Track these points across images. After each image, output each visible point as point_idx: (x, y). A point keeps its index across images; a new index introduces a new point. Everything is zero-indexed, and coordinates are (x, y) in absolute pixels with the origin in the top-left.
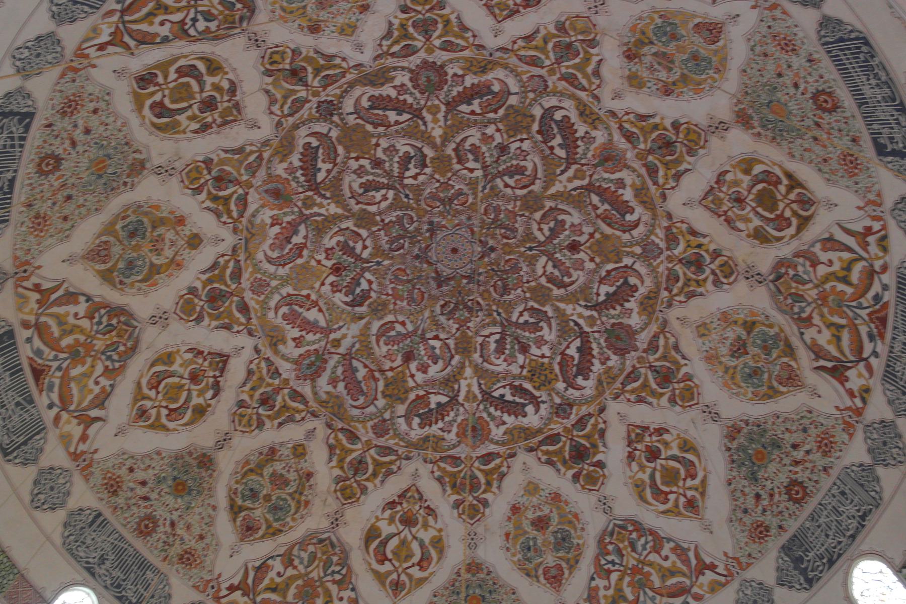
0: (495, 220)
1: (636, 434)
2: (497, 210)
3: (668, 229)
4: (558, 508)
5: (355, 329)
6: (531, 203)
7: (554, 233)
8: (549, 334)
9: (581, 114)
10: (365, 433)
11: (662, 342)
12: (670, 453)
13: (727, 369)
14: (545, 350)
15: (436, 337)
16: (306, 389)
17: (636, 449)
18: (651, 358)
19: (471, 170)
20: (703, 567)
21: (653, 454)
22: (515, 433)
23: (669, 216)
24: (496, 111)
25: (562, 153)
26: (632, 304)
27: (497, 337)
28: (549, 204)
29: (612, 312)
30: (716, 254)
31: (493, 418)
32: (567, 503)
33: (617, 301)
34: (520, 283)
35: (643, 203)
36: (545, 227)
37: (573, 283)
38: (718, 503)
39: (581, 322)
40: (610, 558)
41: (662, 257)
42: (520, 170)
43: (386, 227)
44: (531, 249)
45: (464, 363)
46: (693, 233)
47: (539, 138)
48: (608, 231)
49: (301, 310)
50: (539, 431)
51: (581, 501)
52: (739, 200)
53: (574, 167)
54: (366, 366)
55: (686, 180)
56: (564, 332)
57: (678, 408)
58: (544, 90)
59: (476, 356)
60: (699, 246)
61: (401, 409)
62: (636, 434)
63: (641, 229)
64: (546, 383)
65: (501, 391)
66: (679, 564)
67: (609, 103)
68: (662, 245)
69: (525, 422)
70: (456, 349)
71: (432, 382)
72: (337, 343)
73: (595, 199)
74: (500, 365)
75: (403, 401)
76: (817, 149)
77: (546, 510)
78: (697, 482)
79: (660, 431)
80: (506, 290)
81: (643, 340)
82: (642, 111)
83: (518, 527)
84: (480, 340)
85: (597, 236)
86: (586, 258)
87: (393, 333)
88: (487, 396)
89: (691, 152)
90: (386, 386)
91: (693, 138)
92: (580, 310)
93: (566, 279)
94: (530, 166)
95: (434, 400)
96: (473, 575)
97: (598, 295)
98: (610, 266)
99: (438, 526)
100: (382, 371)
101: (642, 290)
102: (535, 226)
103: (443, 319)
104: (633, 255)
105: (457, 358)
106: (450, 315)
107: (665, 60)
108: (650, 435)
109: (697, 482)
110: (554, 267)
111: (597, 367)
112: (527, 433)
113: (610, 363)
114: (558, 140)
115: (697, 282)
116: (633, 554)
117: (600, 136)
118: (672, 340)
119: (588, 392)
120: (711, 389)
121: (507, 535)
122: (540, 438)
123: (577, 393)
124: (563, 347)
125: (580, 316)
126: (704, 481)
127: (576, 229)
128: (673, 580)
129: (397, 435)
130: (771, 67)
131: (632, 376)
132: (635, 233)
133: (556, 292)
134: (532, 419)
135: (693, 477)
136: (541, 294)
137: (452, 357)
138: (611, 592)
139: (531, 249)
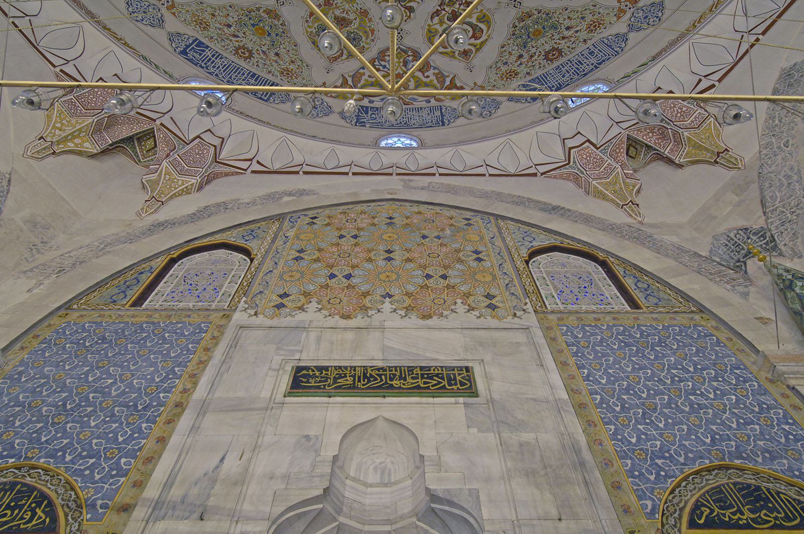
4: (362, 20)
17: (444, 9)
32: (370, 20)
40: (383, 63)
66: (435, 82)
77: (352, 16)
96: (269, 18)
108: (460, 5)
116: (403, 68)
126: (483, 43)
135: (476, 39)
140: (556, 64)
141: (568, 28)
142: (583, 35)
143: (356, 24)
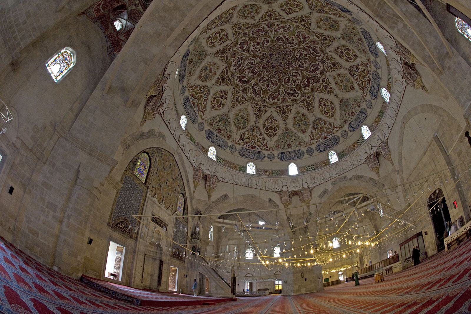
0: (280, 72)
1: (226, 92)
2: (282, 73)
3: (267, 106)
5: (272, 36)
6: (280, 81)
7: (272, 82)
8: (250, 74)
9: (295, 99)
10: (247, 31)
11: (244, 100)
12: (222, 101)
13: (238, 114)
14: (247, 73)
15: (259, 50)
16: (266, 22)
18: (241, 97)
19: (293, 73)
20: (203, 112)
21: (222, 97)
22: (231, 64)
23: (270, 107)
24: (303, 85)
25: (289, 91)
26: (253, 94)
27: (253, 63)
28: (279, 84)
29: (252, 90)
30: (261, 115)
31: (235, 59)
33: (254, 91)
34: (264, 71)
35: (274, 103)
36: (274, 81)
37: (260, 83)
38: (214, 113)
39: (251, 82)
40: (203, 89)
41: (261, 104)
42: (288, 82)
43: (291, 52)
44: (270, 76)
45: (250, 54)
46: (266, 111)
47: (293, 89)
48: (269, 94)
49: (285, 29)
50: (229, 69)
51: (213, 81)
52: (271, 123)
53: (285, 92)
54: (262, 34)
55: (276, 113)
56: (250, 78)
57: (231, 103)
58: (302, 95)
59: (251, 58)
60: (263, 112)
61: (247, 39)
62: (226, 92)
63: (268, 101)
64: (240, 72)
65: (241, 61)
67: (295, 105)
68: (264, 104)
69: (232, 66)
70: (255, 54)
71: (250, 46)
72: (271, 31)
73: (277, 94)
74: (247, 62)
75: (248, 40)
76: (280, 141)
78: (217, 108)
79: (226, 98)
80: (263, 68)
81: (245, 96)
82: (292, 111)
83: (211, 65)
84: (254, 59)
85: (269, 91)
86: (264, 87)
87: (266, 42)
88: (241, 58)
89: (281, 116)
90: (254, 37)
91: (285, 118)
92: (254, 83)
93: (261, 82)
94: (288, 84)
95: (245, 46)
97: (256, 87)
98: (261, 92)
99: (217, 46)
100: (258, 37)
101: (255, 97)
102: (275, 79)
103: (263, 53)
104: (263, 98)
105: (252, 53)
106: (263, 55)
107: (300, 120)
109: (217, 108)
110: (265, 80)
111: (241, 84)
112: (230, 66)
113: (241, 87)
114: (291, 92)
115: (256, 110)
117: (289, 100)
118: (244, 102)
119: (235, 81)
120: (235, 110)
121: (210, 63)
122: (228, 70)
123: (236, 79)
124: (246, 77)
125: (252, 83)
127: (271, 87)
128: (200, 106)
129: (242, 37)
130: (296, 139)
131: (238, 92)
132: (268, 99)
133: (259, 79)
134: (232, 68)
136: (259, 75)
137: (253, 52)
138: (197, 91)
139: (270, 76)
140: (218, 134)
141: (227, 129)
142: (226, 135)
143: (211, 74)
